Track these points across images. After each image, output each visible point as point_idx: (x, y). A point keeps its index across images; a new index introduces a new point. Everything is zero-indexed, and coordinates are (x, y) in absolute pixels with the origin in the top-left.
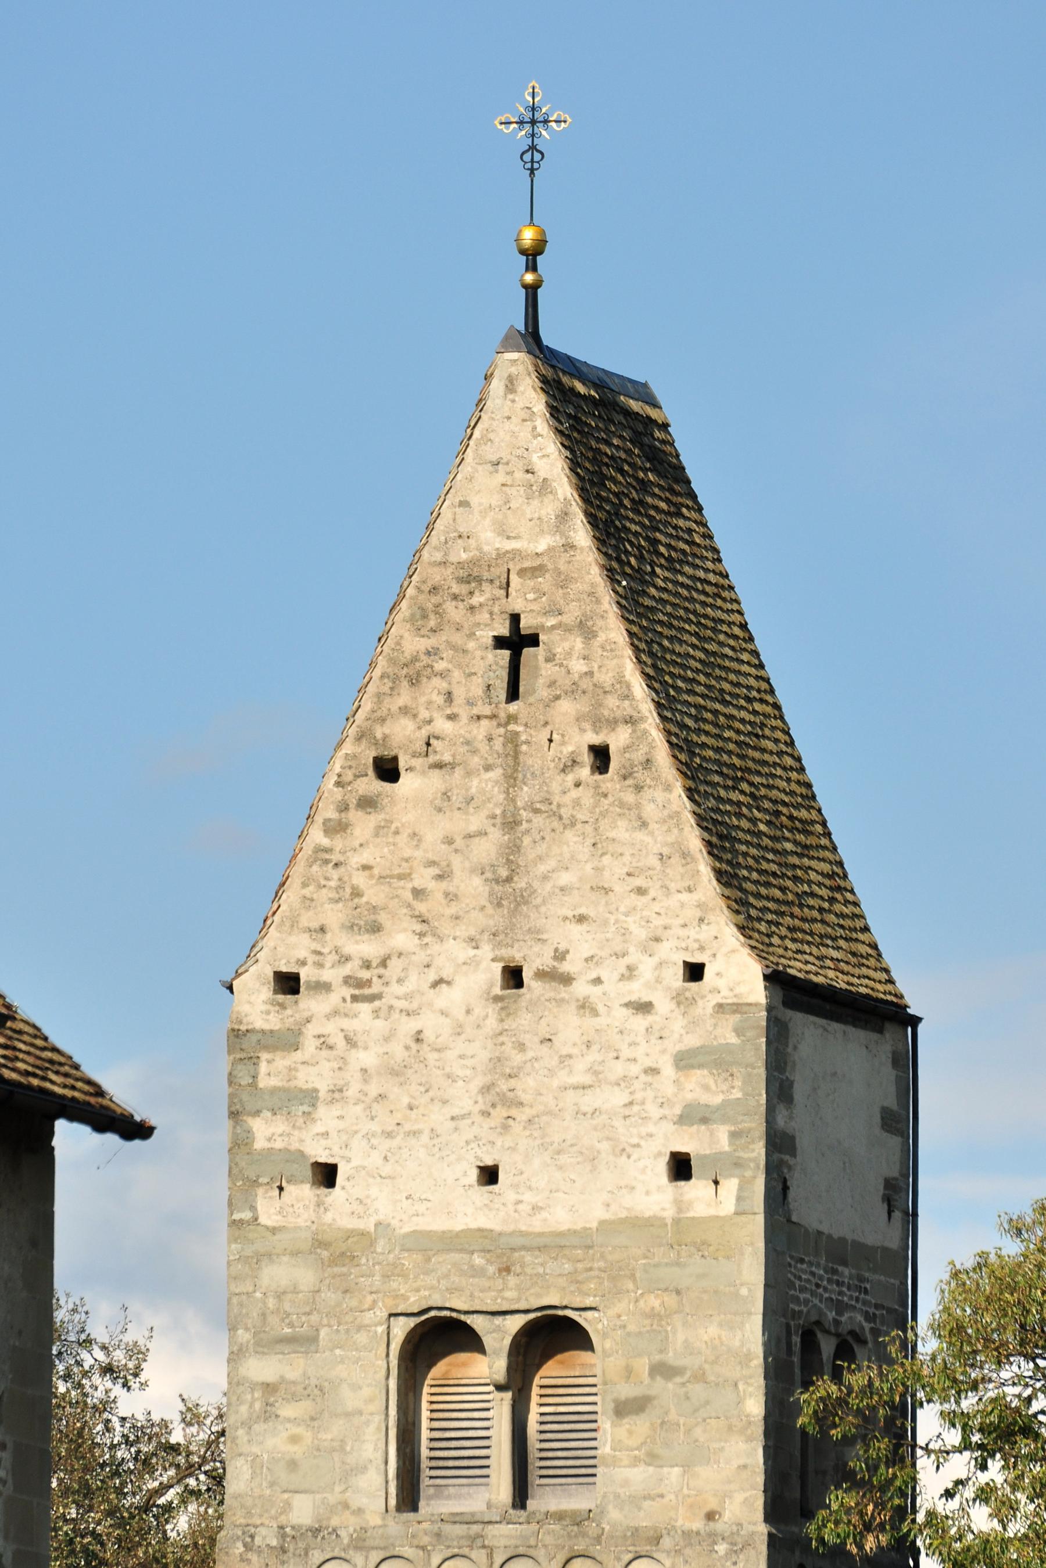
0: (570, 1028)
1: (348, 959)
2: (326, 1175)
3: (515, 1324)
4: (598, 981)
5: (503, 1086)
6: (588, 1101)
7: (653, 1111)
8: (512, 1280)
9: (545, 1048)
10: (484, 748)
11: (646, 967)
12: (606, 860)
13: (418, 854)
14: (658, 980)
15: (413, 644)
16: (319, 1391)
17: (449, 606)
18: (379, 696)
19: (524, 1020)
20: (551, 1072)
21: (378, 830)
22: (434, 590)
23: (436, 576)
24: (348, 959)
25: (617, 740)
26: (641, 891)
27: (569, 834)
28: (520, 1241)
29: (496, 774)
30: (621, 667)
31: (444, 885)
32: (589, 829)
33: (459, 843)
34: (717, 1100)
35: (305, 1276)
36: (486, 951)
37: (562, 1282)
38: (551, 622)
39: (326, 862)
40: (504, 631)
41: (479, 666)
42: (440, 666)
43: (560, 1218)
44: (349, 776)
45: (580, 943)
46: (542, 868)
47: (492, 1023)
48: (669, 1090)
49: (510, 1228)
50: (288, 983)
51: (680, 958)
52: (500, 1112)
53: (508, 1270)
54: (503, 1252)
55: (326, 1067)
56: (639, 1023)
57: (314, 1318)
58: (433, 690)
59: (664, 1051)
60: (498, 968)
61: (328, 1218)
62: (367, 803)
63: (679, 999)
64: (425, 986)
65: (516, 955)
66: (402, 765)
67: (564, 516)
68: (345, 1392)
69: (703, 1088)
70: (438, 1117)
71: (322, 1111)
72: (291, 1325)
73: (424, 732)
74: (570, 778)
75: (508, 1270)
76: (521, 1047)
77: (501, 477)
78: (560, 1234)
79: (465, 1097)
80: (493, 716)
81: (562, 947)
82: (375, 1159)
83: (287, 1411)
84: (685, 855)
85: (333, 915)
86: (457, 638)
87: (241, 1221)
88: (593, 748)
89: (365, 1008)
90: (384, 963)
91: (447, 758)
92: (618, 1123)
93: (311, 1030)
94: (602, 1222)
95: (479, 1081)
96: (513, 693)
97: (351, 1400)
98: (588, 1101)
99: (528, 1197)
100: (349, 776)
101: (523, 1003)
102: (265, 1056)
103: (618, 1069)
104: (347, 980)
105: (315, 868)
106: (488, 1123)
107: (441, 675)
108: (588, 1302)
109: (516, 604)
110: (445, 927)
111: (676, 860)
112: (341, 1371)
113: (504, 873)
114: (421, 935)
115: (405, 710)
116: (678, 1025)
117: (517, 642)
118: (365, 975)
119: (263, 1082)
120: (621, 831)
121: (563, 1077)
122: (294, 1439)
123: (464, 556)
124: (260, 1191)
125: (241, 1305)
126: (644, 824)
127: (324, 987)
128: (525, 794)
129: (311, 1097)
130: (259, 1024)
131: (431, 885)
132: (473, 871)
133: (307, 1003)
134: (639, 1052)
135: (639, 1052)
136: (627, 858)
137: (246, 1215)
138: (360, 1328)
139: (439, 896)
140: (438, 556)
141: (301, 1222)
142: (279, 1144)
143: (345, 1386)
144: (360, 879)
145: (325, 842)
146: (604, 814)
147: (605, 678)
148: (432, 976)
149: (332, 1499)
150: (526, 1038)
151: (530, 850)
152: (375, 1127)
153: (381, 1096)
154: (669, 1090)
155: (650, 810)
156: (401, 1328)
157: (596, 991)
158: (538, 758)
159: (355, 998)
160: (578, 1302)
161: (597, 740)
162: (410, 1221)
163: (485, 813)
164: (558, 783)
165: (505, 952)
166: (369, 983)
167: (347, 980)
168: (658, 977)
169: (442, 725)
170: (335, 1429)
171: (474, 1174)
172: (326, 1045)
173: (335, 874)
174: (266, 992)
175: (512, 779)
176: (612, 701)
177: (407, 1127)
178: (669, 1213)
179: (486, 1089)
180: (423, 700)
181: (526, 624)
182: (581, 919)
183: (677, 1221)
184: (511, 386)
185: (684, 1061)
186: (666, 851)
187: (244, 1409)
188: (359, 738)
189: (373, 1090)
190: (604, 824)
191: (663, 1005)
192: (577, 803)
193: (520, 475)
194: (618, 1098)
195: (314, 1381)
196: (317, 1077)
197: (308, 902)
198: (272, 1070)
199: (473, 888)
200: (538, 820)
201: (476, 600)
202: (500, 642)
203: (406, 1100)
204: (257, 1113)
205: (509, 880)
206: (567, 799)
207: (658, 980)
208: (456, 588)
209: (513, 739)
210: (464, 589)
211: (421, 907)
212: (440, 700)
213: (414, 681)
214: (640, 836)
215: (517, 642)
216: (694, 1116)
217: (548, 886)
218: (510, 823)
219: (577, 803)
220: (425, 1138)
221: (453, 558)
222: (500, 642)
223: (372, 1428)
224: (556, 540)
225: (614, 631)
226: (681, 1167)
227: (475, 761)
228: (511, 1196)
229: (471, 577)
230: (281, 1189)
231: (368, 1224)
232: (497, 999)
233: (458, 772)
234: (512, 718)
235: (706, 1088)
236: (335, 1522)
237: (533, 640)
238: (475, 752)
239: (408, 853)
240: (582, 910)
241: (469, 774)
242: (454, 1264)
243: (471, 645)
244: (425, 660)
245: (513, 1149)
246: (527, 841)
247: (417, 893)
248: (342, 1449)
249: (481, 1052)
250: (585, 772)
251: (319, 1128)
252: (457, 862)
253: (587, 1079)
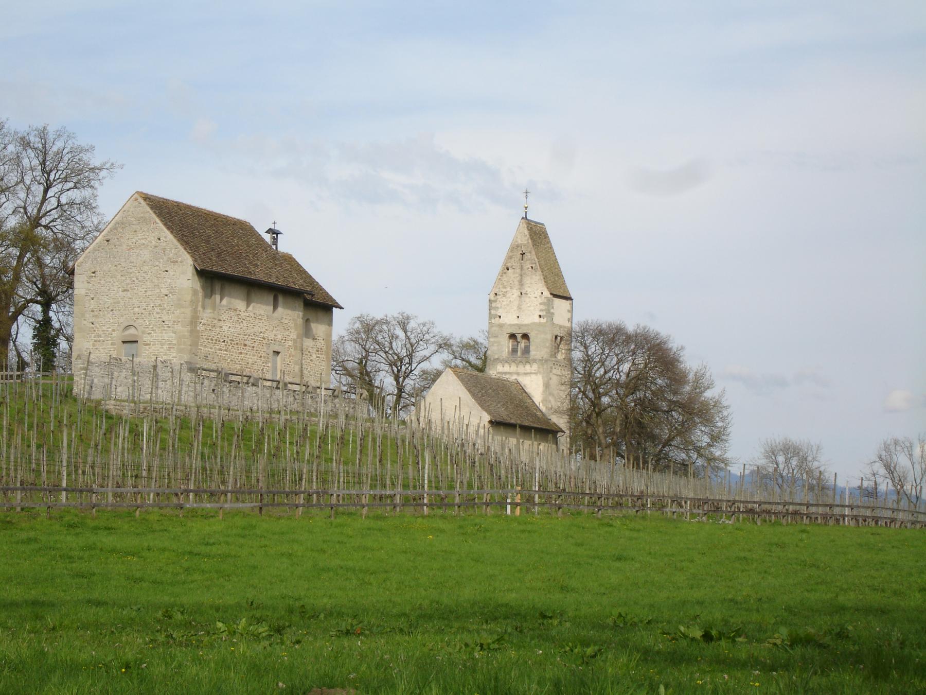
43: (526, 322)
45: (529, 290)
54: (519, 326)
69: (543, 307)
79: (515, 308)
117: (523, 254)
168: (538, 293)
185: (541, 304)
196: (499, 306)
198: (494, 305)
199: (517, 283)
215: (523, 254)
216: (541, 310)
226: (540, 316)
229: (518, 246)
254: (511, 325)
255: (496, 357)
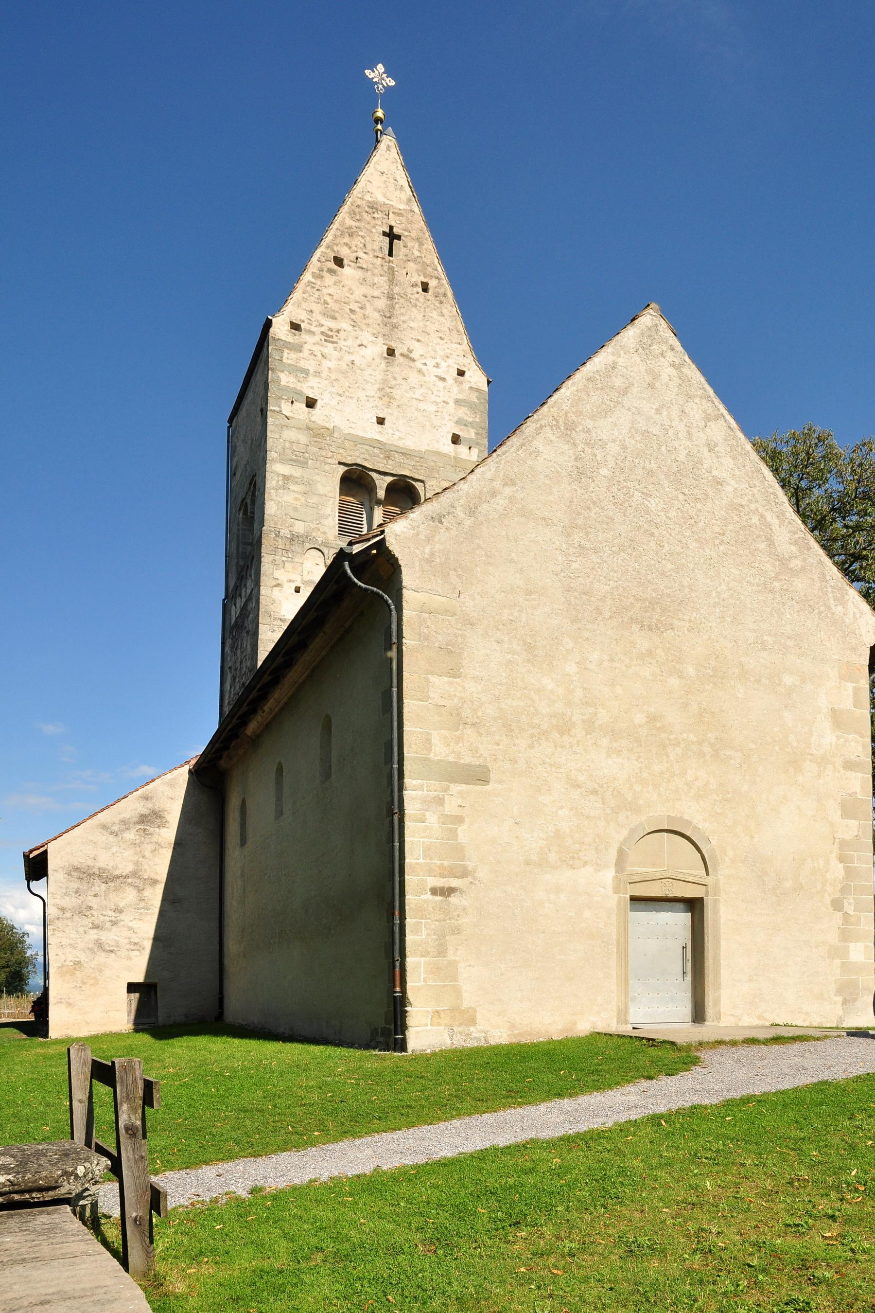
0: (414, 378)
1: (322, 325)
2: (311, 403)
3: (389, 479)
4: (425, 364)
5: (389, 390)
6: (422, 406)
7: (447, 418)
8: (390, 462)
9: (403, 382)
10: (380, 268)
11: (443, 365)
12: (428, 323)
13: (352, 297)
14: (448, 371)
15: (349, 222)
16: (309, 483)
17: (365, 214)
18: (335, 236)
19: (396, 369)
20: (407, 391)
21: (335, 283)
22: (358, 206)
23: (359, 202)
24: (322, 325)
25: (432, 283)
26: (441, 338)
27: (414, 309)
28: (393, 448)
29: (385, 278)
30: (433, 259)
31: (363, 311)
32: (422, 310)
33: (369, 298)
34: (471, 420)
35: (303, 439)
36: (381, 340)
37: (411, 468)
38: (406, 234)
39: (314, 287)
40: (388, 231)
41: (376, 238)
42: (360, 233)
43: (410, 443)
44: (323, 259)
45: (418, 351)
46: (403, 318)
47: (383, 366)
48: (453, 411)
49: (391, 443)
50: (295, 327)
51: (456, 367)
52: (386, 399)
53: (389, 457)
54: (388, 452)
55: (312, 362)
56: (441, 384)
57: (306, 455)
58: (357, 242)
59: (450, 397)
60: (385, 348)
61: (313, 419)
62: (330, 271)
63: (455, 379)
64: (356, 345)
65: (393, 345)
66: (345, 262)
67: (409, 200)
68: (319, 486)
70: (361, 394)
71: (311, 378)
72: (296, 455)
73: (355, 255)
74: (415, 289)
75: (389, 457)
76: (395, 379)
77: (384, 178)
78: (410, 450)
79: (372, 390)
80: (383, 258)
81: (411, 348)
82: (334, 402)
83: (293, 487)
84: (458, 331)
85: (317, 308)
86: (367, 226)
87: (274, 411)
88: (422, 283)
89: (330, 345)
90: (338, 331)
91: (364, 266)
92: (433, 417)
93: (306, 347)
94: (427, 450)
95: (377, 386)
96: (391, 254)
97: (321, 489)
98: (422, 406)
99: (397, 433)
100: (323, 259)
101: (396, 363)
102: (286, 351)
103: (433, 398)
104: (322, 333)
105: (308, 288)
106: (381, 402)
107: (363, 237)
108: (420, 478)
109: (393, 224)
110: (364, 327)
111: (455, 332)
112: (318, 478)
113: (388, 315)
114: (354, 326)
115: (346, 244)
116: (455, 389)
118: (330, 333)
119: (285, 360)
120: (435, 314)
121: (410, 394)
122: (296, 499)
123: (370, 199)
124: (283, 401)
125: (273, 442)
126: (443, 315)
127: (312, 333)
128: (396, 289)
129: (306, 372)
130: (283, 338)
131: (358, 310)
132: (375, 310)
133: (304, 337)
134: (441, 394)
135: (441, 394)
136: (436, 325)
137: (277, 409)
138: (326, 463)
139: (361, 315)
140: (360, 196)
141: (301, 417)
142: (291, 385)
143: (319, 484)
144: (328, 299)
145: (313, 280)
146: (428, 307)
147: (428, 262)
148: (359, 342)
149: (312, 526)
150: (397, 376)
151: (398, 311)
152: (334, 390)
153: (336, 380)
154: (453, 411)
155: (445, 311)
156: (342, 469)
157: (424, 368)
158: (400, 275)
159: (326, 341)
160: (416, 477)
161: (425, 280)
162: (346, 428)
163: (380, 291)
164: (409, 290)
165: (387, 342)
166: (332, 337)
167: (322, 333)
169: (361, 254)
170: (314, 500)
171: (375, 420)
172: (312, 353)
173: (317, 293)
174: (288, 327)
175: (392, 281)
176: (430, 269)
177: (347, 394)
178: (452, 454)
179: (380, 390)
180: (354, 243)
181: (396, 231)
182: (418, 341)
183: (455, 458)
184: (388, 148)
185: (457, 402)
186: (451, 328)
187: (274, 482)
188: (328, 247)
189: (333, 376)
190: (427, 310)
191: (450, 381)
192: (417, 299)
193: (392, 180)
194: (432, 408)
195: (305, 479)
196: (310, 365)
197: (305, 300)
200: (402, 300)
201: (376, 215)
202: (384, 234)
203: (347, 384)
204: (282, 371)
205: (390, 317)
206: (413, 297)
207: (448, 371)
208: (367, 209)
209: (391, 269)
210: (371, 211)
211: (353, 317)
212: (362, 246)
213: (351, 235)
214: (441, 319)
215: (392, 236)
217: (405, 326)
218: (391, 298)
219: (417, 299)
220: (355, 400)
221: (365, 198)
222: (384, 234)
223: (331, 502)
224: (407, 207)
225: (429, 245)
226: (456, 439)
227: (376, 271)
228: (390, 432)
229: (373, 207)
230: (292, 402)
231: (331, 426)
232: (385, 358)
233: (369, 273)
234: (390, 261)
235: (466, 414)
236: (314, 534)
237: (399, 237)
238: (376, 268)
239: (348, 295)
240: (419, 338)
241: (374, 275)
242: (367, 450)
243: (374, 230)
244: (355, 229)
245: (392, 414)
246: (397, 306)
247: (352, 311)
248: (317, 508)
249: (379, 376)
250: (420, 290)
251: (309, 384)
252: (368, 305)
253: (421, 398)
254: (358, 441)
255: (299, 528)
